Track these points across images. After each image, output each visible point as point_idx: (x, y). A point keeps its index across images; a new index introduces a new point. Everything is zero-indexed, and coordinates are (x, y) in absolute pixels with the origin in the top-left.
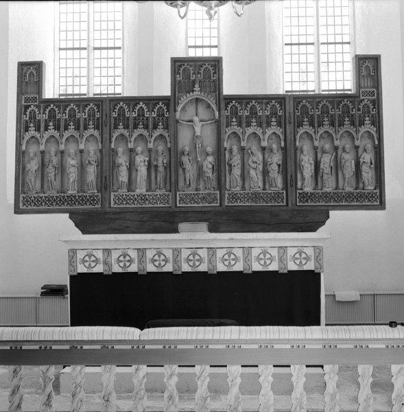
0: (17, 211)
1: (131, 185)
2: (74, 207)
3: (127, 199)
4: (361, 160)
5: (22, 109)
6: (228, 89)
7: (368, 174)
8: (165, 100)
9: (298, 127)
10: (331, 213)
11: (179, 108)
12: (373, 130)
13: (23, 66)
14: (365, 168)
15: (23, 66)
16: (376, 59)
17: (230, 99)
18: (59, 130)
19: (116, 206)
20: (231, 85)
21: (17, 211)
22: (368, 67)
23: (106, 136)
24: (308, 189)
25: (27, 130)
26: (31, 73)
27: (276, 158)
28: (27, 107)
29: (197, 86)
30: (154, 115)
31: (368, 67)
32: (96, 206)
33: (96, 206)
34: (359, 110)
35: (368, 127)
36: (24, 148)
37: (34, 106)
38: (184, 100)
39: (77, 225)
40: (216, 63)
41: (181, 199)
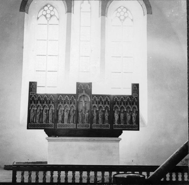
0: (28, 128)
1: (63, 121)
2: (45, 128)
3: (61, 126)
4: (132, 115)
5: (30, 96)
6: (94, 92)
7: (134, 120)
8: (74, 95)
9: (114, 105)
10: (123, 131)
11: (78, 98)
12: (136, 107)
13: (31, 83)
14: (133, 118)
15: (31, 83)
16: (137, 85)
17: (93, 96)
18: (41, 103)
19: (58, 128)
20: (95, 91)
21: (28, 128)
22: (136, 88)
23: (56, 106)
24: (116, 124)
25: (31, 103)
26: (33, 86)
27: (107, 114)
28: (31, 96)
29: (84, 91)
30: (71, 99)
31: (136, 88)
32: (52, 127)
33: (52, 127)
34: (132, 100)
35: (135, 105)
36: (30, 109)
37: (34, 95)
38: (80, 95)
39: (46, 133)
40: (90, 84)
41: (78, 126)
